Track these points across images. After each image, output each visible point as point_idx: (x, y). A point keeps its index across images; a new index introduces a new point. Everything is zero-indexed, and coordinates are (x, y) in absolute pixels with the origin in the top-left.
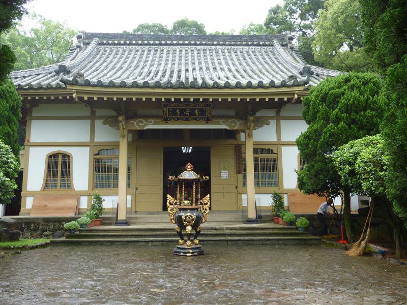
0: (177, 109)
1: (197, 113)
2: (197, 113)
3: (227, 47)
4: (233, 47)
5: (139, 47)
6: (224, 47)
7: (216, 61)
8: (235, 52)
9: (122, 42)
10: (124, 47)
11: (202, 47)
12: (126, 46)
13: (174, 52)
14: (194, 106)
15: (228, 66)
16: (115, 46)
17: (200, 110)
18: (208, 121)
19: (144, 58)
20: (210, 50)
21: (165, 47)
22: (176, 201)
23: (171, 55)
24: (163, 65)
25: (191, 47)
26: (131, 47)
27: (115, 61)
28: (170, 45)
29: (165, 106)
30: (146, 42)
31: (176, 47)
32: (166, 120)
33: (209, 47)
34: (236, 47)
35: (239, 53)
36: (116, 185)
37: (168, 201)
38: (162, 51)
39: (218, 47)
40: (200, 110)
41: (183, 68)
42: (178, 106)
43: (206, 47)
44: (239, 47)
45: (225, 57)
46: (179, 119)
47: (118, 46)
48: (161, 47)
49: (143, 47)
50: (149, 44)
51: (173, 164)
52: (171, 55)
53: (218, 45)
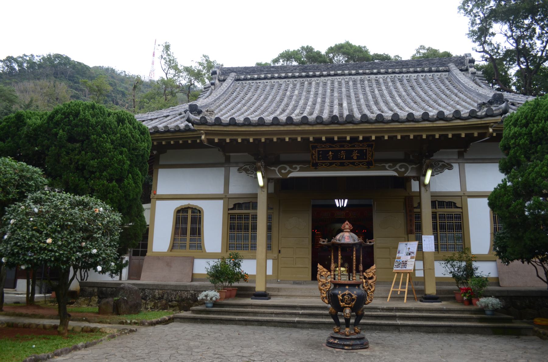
0: (328, 151)
1: (355, 155)
2: (355, 155)
3: (390, 76)
4: (397, 75)
5: (281, 81)
6: (386, 76)
7: (377, 92)
8: (401, 81)
9: (263, 76)
10: (265, 81)
11: (359, 77)
12: (267, 81)
13: (325, 84)
14: (350, 147)
15: (392, 97)
16: (254, 81)
17: (360, 151)
18: (369, 166)
19: (288, 93)
20: (369, 80)
21: (313, 79)
22: (329, 273)
23: (321, 88)
24: (311, 100)
25: (345, 77)
26: (272, 81)
27: (254, 98)
28: (320, 76)
29: (314, 147)
30: (290, 74)
31: (326, 78)
32: (315, 167)
33: (367, 76)
34: (401, 75)
35: (405, 81)
38: (310, 84)
39: (379, 76)
40: (360, 151)
41: (336, 102)
42: (331, 147)
43: (363, 77)
44: (405, 75)
45: (387, 88)
46: (331, 164)
47: (258, 81)
48: (309, 79)
49: (286, 80)
50: (294, 77)
51: (324, 224)
52: (321, 88)
53: (379, 73)
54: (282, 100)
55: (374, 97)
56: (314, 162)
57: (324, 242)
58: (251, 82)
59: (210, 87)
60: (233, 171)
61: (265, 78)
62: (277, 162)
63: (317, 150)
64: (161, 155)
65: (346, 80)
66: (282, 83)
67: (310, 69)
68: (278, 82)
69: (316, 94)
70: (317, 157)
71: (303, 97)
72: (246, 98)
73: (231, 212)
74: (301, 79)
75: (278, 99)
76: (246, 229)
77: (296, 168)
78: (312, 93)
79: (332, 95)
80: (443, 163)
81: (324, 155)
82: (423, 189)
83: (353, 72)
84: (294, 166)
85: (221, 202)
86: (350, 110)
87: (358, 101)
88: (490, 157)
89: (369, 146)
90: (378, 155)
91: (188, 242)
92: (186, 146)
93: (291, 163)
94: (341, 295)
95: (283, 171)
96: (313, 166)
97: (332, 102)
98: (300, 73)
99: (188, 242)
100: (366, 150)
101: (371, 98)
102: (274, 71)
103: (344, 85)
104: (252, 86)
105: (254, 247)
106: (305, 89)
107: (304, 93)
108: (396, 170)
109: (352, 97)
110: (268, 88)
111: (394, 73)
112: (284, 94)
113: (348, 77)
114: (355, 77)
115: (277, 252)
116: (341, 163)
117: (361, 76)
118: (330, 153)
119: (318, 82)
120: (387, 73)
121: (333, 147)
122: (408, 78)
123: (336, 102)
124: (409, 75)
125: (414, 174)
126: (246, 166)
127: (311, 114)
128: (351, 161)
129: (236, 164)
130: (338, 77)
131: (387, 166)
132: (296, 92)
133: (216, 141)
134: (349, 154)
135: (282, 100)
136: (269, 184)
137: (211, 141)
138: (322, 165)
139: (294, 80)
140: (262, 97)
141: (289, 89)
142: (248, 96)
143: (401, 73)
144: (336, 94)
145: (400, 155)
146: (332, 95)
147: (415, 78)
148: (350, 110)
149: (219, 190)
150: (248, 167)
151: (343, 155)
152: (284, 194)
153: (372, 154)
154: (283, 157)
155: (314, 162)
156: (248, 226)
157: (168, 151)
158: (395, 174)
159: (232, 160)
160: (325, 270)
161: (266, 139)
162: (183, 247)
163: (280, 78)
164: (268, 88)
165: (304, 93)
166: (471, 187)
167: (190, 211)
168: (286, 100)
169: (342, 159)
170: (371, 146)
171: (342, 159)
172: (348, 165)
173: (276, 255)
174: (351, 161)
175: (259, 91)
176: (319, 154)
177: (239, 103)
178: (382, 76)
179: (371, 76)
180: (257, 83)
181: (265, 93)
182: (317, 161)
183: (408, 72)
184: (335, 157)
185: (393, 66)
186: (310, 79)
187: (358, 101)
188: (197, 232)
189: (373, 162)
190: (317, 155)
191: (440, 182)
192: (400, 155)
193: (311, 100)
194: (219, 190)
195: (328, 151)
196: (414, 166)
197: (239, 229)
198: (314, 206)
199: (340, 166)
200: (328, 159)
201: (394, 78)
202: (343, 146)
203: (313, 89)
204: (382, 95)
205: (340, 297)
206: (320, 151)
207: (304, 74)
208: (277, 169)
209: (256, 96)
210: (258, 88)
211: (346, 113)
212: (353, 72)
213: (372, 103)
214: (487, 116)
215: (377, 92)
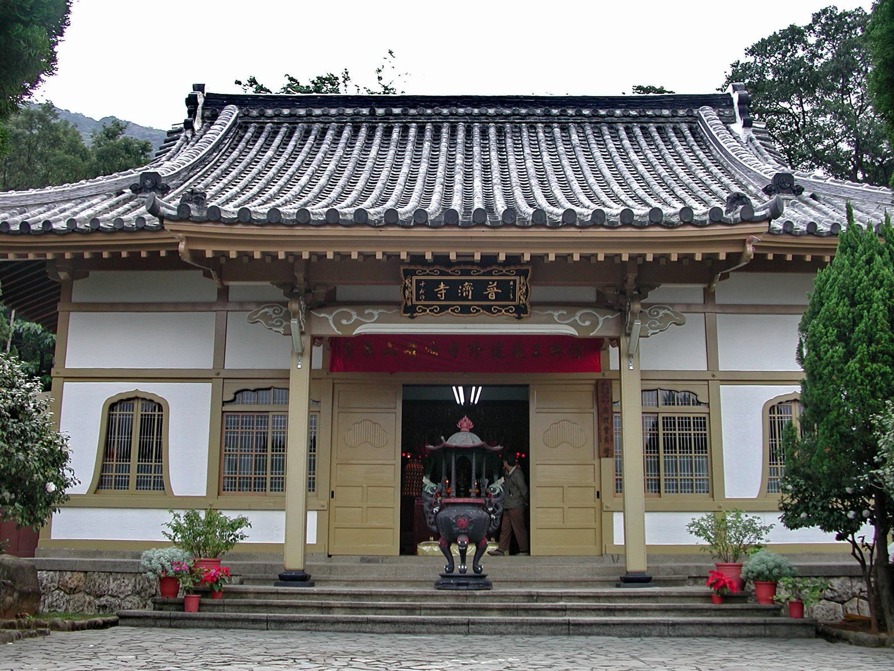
0: (439, 282)
1: (492, 292)
2: (492, 292)
17: (500, 284)
18: (521, 313)
24: (405, 170)
29: (409, 273)
32: (411, 311)
40: (500, 284)
42: (443, 273)
46: (443, 308)
56: (409, 303)
59: (180, 131)
60: (237, 322)
62: (330, 302)
63: (415, 278)
64: (76, 283)
73: (228, 408)
77: (371, 315)
80: (666, 311)
81: (429, 291)
82: (624, 361)
84: (366, 312)
85: (206, 388)
88: (748, 302)
89: (519, 273)
90: (538, 293)
91: (133, 475)
92: (135, 263)
93: (359, 304)
95: (344, 322)
96: (405, 312)
99: (133, 475)
100: (515, 281)
105: (279, 485)
108: (574, 325)
115: (327, 494)
118: (442, 286)
125: (611, 333)
126: (266, 310)
129: (242, 305)
131: (556, 314)
133: (209, 254)
134: (480, 291)
136: (314, 348)
137: (198, 256)
138: (424, 311)
145: (588, 294)
148: (488, 196)
149: (206, 362)
150: (270, 311)
151: (468, 289)
153: (527, 290)
154: (343, 292)
155: (409, 303)
157: (92, 273)
158: (572, 331)
159: (232, 296)
161: (311, 254)
162: (122, 483)
166: (726, 364)
167: (138, 405)
169: (466, 299)
170: (524, 273)
171: (466, 299)
172: (478, 311)
173: (325, 503)
176: (418, 288)
182: (415, 302)
184: (452, 294)
188: (153, 450)
189: (528, 306)
191: (663, 352)
192: (588, 294)
193: (405, 170)
194: (206, 362)
199: (460, 312)
208: (330, 318)
211: (478, 203)
214: (744, 221)
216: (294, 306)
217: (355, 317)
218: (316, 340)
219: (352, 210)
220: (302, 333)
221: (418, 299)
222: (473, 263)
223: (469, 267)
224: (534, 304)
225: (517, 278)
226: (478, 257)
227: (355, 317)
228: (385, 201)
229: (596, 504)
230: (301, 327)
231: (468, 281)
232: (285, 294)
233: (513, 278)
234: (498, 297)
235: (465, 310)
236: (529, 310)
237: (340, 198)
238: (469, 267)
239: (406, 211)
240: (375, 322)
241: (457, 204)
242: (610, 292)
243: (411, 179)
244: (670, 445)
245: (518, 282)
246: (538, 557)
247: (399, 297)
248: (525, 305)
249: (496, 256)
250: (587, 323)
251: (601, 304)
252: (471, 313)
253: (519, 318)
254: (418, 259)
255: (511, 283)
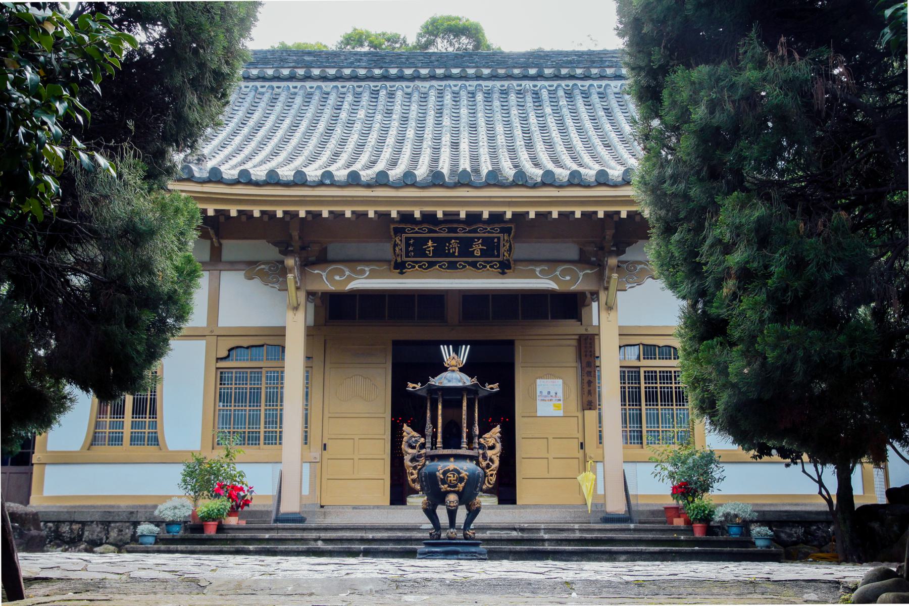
0: (426, 240)
1: (477, 248)
2: (477, 248)
3: (563, 83)
4: (579, 83)
5: (327, 86)
6: (555, 83)
7: (533, 119)
8: (586, 95)
9: (286, 72)
10: (291, 84)
11: (498, 84)
12: (295, 84)
13: (424, 97)
14: (469, 232)
15: (563, 130)
16: (267, 84)
17: (485, 241)
18: (505, 268)
19: (344, 115)
20: (519, 92)
21: (397, 84)
22: (422, 440)
23: (414, 107)
24: (393, 132)
25: (467, 83)
26: (308, 84)
27: (269, 124)
28: (413, 78)
29: (398, 231)
30: (347, 72)
31: (427, 84)
32: (400, 268)
33: (515, 83)
34: (587, 83)
35: (595, 98)
36: (274, 438)
37: (405, 439)
38: (391, 95)
39: (539, 83)
40: (485, 241)
41: (446, 139)
42: (431, 231)
43: (506, 83)
44: (595, 83)
45: (556, 110)
46: (431, 264)
47: (275, 84)
48: (388, 84)
49: (339, 84)
50: (355, 78)
52: (414, 107)
53: (540, 76)
54: (329, 131)
55: (526, 131)
56: (399, 260)
57: (414, 388)
58: (258, 84)
61: (292, 78)
63: (404, 236)
65: (469, 88)
66: (329, 90)
67: (391, 62)
68: (319, 87)
69: (405, 120)
70: (404, 250)
71: (377, 126)
72: (251, 123)
74: (372, 84)
75: (321, 127)
76: (255, 397)
77: (363, 272)
78: (394, 116)
79: (438, 123)
83: (486, 71)
86: (475, 158)
87: (492, 138)
93: (352, 261)
94: (441, 471)
95: (337, 278)
96: (395, 268)
97: (437, 139)
98: (369, 68)
100: (499, 238)
101: (520, 132)
102: (311, 62)
103: (464, 101)
104: (263, 94)
106: (380, 107)
107: (379, 117)
109: (480, 129)
110: (298, 100)
111: (572, 77)
112: (335, 118)
113: (475, 83)
114: (490, 83)
116: (449, 262)
117: (503, 83)
118: (430, 243)
119: (409, 90)
120: (557, 77)
121: (435, 232)
122: (601, 90)
123: (446, 139)
124: (604, 83)
127: (394, 163)
128: (470, 260)
130: (452, 83)
132: (361, 114)
134: (466, 246)
135: (329, 131)
139: (355, 84)
140: (287, 122)
141: (346, 106)
142: (257, 116)
143: (586, 77)
144: (447, 121)
146: (438, 123)
147: (617, 90)
148: (475, 158)
151: (454, 246)
152: (339, 318)
153: (510, 246)
154: (334, 250)
155: (399, 260)
156: (259, 395)
160: (415, 434)
163: (324, 78)
164: (298, 100)
165: (379, 117)
168: (338, 131)
170: (507, 231)
171: (453, 255)
174: (470, 260)
175: (278, 107)
176: (408, 245)
177: (235, 133)
178: (546, 83)
179: (524, 83)
180: (273, 88)
181: (293, 112)
182: (405, 259)
183: (602, 77)
185: (571, 62)
186: (392, 83)
187: (492, 138)
189: (512, 262)
190: (403, 246)
195: (426, 240)
196: (589, 271)
197: (240, 398)
198: (396, 344)
199: (448, 268)
200: (426, 256)
201: (572, 89)
202: (454, 230)
203: (398, 109)
204: (543, 128)
205: (440, 475)
206: (410, 239)
207: (377, 72)
208: (324, 275)
209: (272, 118)
210: (274, 99)
212: (486, 71)
213: (520, 143)
215: (533, 119)
216: (290, 262)
217: (347, 273)
218: (310, 294)
219: (346, 172)
220: (298, 289)
221: (407, 256)
222: (459, 221)
223: (455, 226)
224: (515, 261)
225: (501, 235)
226: (463, 215)
227: (347, 273)
228: (374, 163)
229: (580, 454)
230: (296, 282)
231: (455, 238)
232: (281, 252)
233: (498, 235)
234: (484, 253)
235: (452, 266)
236: (512, 266)
237: (333, 161)
238: (455, 226)
239: (395, 174)
240: (366, 278)
241: (445, 167)
242: (592, 248)
243: (400, 141)
244: (651, 397)
245: (502, 239)
246: (525, 507)
247: (389, 255)
248: (508, 260)
249: (481, 214)
250: (568, 278)
251: (583, 260)
252: (458, 268)
253: (503, 273)
254: (407, 218)
255: (496, 240)
